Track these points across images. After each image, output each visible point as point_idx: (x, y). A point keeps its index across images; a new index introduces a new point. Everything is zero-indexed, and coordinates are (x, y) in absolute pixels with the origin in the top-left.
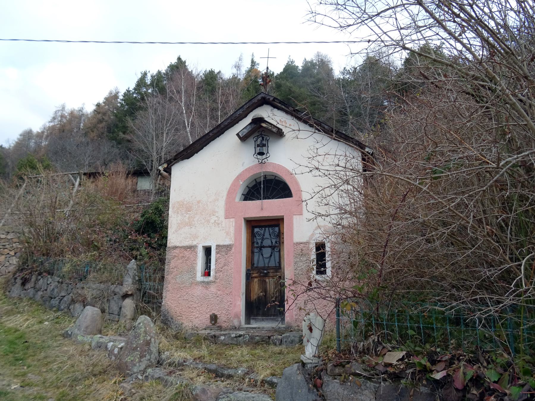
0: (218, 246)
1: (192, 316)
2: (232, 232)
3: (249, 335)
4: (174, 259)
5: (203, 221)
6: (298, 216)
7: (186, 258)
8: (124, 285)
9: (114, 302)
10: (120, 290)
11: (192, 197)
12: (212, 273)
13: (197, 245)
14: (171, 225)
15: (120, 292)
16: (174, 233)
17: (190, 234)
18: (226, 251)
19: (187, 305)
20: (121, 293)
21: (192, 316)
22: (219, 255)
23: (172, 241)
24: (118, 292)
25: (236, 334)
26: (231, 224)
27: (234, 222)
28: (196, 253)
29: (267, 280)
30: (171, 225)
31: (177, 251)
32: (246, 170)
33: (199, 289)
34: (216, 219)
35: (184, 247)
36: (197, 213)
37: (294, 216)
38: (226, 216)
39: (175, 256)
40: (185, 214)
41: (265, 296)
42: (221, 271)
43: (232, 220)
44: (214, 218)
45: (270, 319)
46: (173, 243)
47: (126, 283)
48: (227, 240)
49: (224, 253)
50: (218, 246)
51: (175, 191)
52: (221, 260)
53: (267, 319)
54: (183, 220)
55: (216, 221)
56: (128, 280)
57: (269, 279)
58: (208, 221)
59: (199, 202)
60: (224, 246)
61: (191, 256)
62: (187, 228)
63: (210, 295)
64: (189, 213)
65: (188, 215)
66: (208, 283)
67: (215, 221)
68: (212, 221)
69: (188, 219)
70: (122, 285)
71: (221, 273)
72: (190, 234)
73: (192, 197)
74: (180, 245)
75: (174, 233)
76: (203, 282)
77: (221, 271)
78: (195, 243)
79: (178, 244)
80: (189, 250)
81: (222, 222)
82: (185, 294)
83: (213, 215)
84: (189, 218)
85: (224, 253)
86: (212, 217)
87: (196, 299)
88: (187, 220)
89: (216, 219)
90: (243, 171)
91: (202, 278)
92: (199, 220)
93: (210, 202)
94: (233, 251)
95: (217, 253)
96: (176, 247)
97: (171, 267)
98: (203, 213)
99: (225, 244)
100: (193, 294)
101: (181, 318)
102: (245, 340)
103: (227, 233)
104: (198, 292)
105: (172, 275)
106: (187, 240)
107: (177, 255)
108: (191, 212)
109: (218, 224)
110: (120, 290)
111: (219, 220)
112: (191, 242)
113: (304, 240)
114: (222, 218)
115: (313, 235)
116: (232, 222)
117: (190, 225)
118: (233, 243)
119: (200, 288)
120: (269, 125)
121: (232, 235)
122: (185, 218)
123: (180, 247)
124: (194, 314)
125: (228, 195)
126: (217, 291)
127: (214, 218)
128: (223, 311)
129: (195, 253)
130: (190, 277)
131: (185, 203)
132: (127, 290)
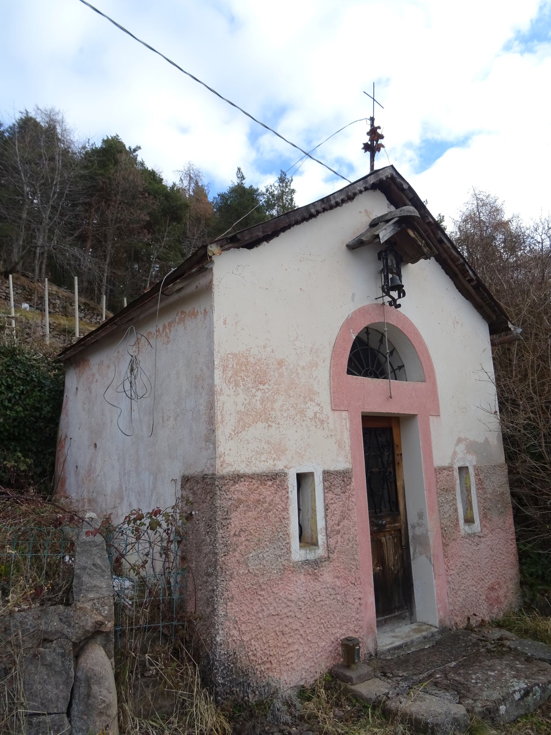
0: (327, 474)
1: (291, 655)
2: (347, 441)
3: (538, 685)
4: (238, 509)
5: (293, 412)
6: (434, 418)
7: (265, 505)
8: (79, 605)
9: (41, 669)
10: (66, 620)
11: (265, 347)
12: (321, 538)
13: (286, 470)
14: (222, 415)
15: (67, 630)
16: (231, 437)
17: (269, 443)
18: (343, 484)
19: (277, 629)
20: (74, 634)
21: (291, 655)
22: (330, 495)
23: (228, 459)
24: (57, 632)
25: (519, 691)
26: (344, 424)
27: (348, 420)
28: (286, 489)
29: (383, 539)
30: (222, 415)
31: (242, 487)
32: (359, 310)
33: (299, 582)
34: (317, 409)
35: (258, 475)
36: (277, 390)
37: (431, 418)
38: (335, 405)
39: (240, 501)
40: (254, 390)
41: (383, 571)
42: (338, 532)
43: (345, 414)
44: (311, 409)
45: (395, 617)
46: (229, 464)
47: (91, 596)
48: (340, 459)
49: (338, 490)
50: (327, 474)
51: (225, 323)
52: (334, 505)
53: (390, 619)
54: (249, 404)
55: (318, 415)
56: (94, 583)
57: (385, 536)
58: (302, 413)
59: (281, 363)
60: (338, 473)
61: (277, 499)
62: (260, 425)
63: (323, 592)
64: (261, 387)
65: (259, 394)
66: (316, 563)
67: (315, 414)
68: (310, 414)
69: (261, 404)
70: (68, 604)
71: (339, 536)
72: (269, 443)
73: (265, 347)
74: (249, 471)
75: (231, 437)
76: (307, 562)
77: (338, 532)
78: (280, 466)
79: (243, 469)
80: (270, 483)
81: (328, 418)
82: (271, 599)
83: (311, 400)
84: (262, 401)
85: (338, 490)
86: (309, 403)
87: (296, 610)
88: (259, 406)
89: (317, 409)
90: (355, 312)
91: (303, 552)
92: (285, 408)
93: (303, 368)
94: (353, 484)
95: (327, 489)
96: (237, 478)
97: (232, 533)
98: (292, 393)
99: (337, 469)
100: (290, 597)
101: (268, 665)
102: (536, 698)
103: (340, 444)
104: (298, 590)
105: (236, 554)
106: (263, 458)
107: (243, 498)
108: (267, 386)
109: (322, 422)
110: (66, 620)
111: (322, 413)
112: (271, 462)
113: (446, 463)
114: (327, 409)
115: (455, 453)
116: (345, 419)
117: (267, 420)
118: (350, 466)
119: (302, 577)
120: (419, 238)
121: (348, 448)
122: (254, 401)
123: (251, 477)
124: (296, 647)
125: (332, 358)
126: (336, 580)
127: (311, 409)
128: (349, 625)
129: (284, 492)
130: (278, 552)
131: (251, 360)
132: (100, 618)
